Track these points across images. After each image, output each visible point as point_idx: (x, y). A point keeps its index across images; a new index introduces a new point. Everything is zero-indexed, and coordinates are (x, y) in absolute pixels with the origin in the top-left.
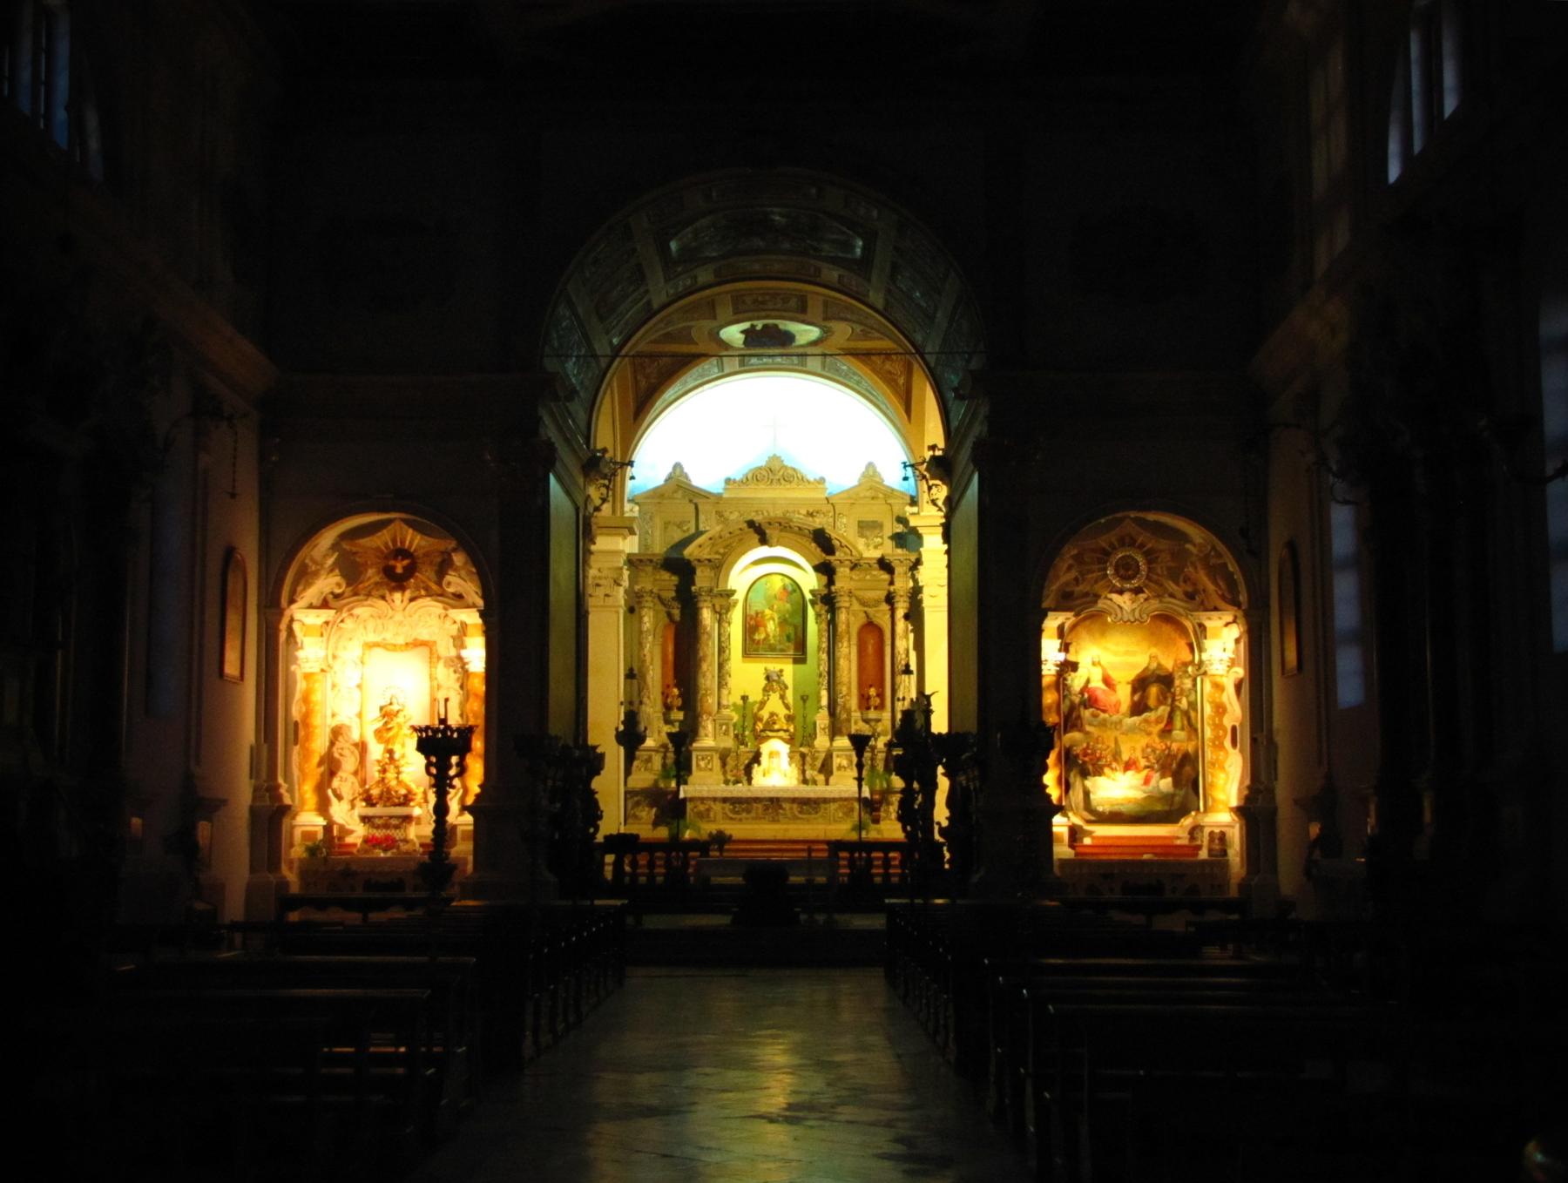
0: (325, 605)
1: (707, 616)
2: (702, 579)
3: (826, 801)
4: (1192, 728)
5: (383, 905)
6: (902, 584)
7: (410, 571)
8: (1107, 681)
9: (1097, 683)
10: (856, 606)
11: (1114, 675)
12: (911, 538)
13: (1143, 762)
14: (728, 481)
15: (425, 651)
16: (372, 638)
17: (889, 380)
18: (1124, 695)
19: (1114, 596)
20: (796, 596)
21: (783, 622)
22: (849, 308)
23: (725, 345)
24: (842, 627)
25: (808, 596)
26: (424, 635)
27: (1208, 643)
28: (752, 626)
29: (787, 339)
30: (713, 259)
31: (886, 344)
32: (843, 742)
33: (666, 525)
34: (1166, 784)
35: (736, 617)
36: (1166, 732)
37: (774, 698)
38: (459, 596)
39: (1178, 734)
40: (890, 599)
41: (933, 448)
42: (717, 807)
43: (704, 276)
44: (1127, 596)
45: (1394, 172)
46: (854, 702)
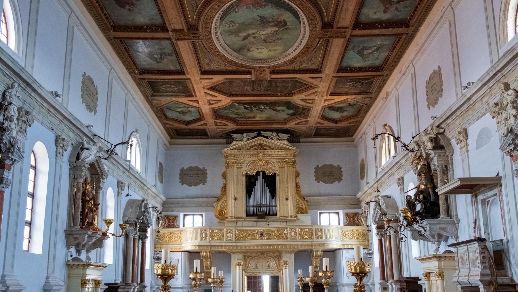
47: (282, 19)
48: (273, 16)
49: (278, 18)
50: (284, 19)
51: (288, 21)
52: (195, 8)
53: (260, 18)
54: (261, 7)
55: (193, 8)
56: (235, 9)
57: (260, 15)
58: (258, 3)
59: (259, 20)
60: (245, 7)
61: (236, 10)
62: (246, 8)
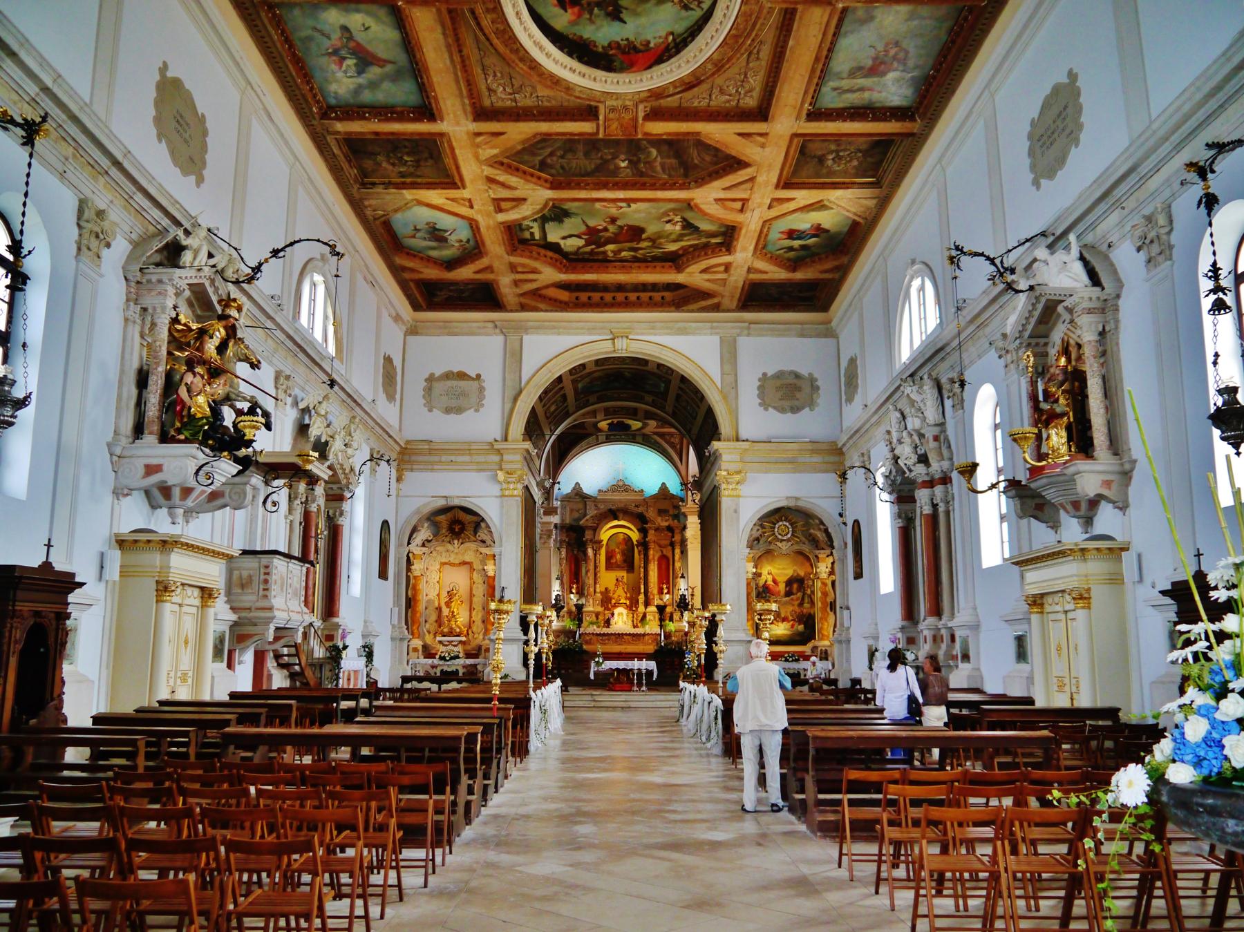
0: (423, 545)
1: (590, 551)
2: (588, 535)
3: (644, 635)
4: (812, 603)
5: (448, 682)
6: (677, 538)
7: (463, 530)
8: (774, 581)
9: (770, 582)
10: (657, 548)
11: (779, 579)
12: (682, 518)
13: (791, 618)
14: (600, 491)
15: (467, 567)
16: (444, 560)
17: (673, 446)
18: (782, 587)
19: (778, 544)
20: (629, 543)
21: (623, 554)
22: (656, 414)
23: (600, 430)
24: (651, 557)
25: (635, 543)
26: (467, 559)
27: (819, 564)
28: (609, 557)
29: (628, 427)
30: (598, 392)
31: (673, 430)
32: (654, 609)
33: (572, 510)
34: (801, 628)
35: (603, 551)
36: (801, 605)
37: (620, 588)
38: (483, 542)
39: (806, 605)
40: (672, 545)
41: (694, 476)
42: (594, 638)
43: (592, 399)
44: (784, 543)
45: (905, 354)
46: (655, 591)
47: (569, 11)
48: (591, 21)
49: (579, 16)
50: (566, 11)
51: (555, 6)
52: (755, 51)
53: (621, 15)
54: (618, 43)
55: (758, 52)
56: (674, 40)
57: (622, 24)
58: (624, 53)
59: (624, 11)
60: (652, 45)
61: (671, 38)
62: (649, 42)
